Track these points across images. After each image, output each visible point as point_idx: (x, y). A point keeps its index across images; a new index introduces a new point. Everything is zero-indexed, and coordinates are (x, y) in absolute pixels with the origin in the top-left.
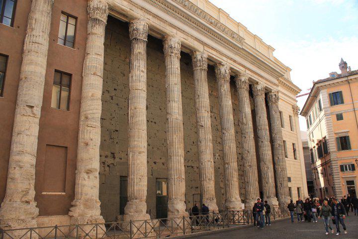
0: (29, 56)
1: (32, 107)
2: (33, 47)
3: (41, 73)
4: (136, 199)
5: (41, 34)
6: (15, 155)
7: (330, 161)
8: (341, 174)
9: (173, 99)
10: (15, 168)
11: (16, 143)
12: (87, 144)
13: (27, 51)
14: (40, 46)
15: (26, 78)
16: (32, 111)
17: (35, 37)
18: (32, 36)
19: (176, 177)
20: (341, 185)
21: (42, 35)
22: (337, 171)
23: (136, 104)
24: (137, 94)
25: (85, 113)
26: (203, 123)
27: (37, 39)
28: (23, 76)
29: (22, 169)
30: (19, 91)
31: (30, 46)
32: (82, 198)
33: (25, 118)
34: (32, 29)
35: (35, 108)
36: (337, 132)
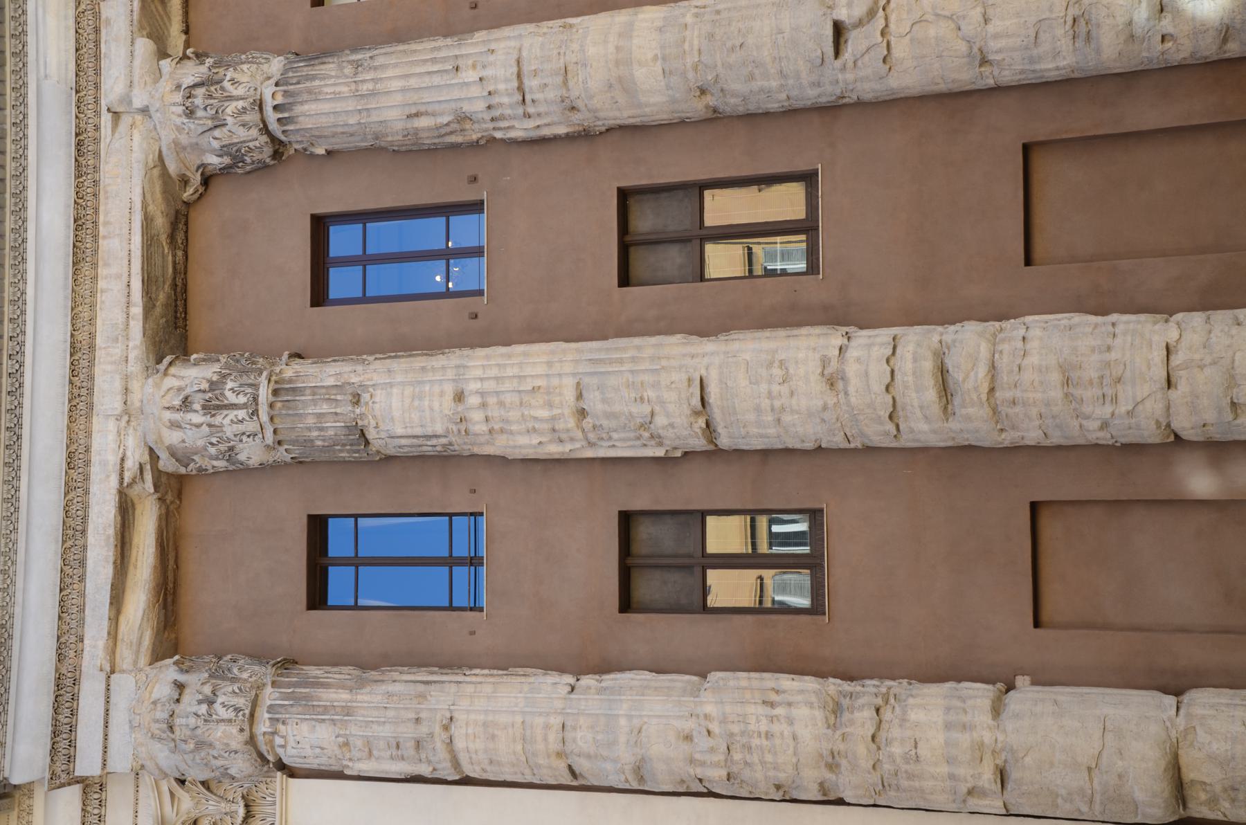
0: (596, 103)
1: (839, 30)
2: (545, 93)
3: (660, 30)
5: (470, 76)
6: (1098, 51)
10: (1163, 37)
11: (1032, 60)
13: (576, 117)
14: (526, 68)
15: (703, 91)
16: (860, 23)
17: (495, 100)
18: (496, 113)
21: (474, 66)
27: (502, 87)
28: (696, 108)
30: (773, 106)
31: (542, 109)
33: (899, 51)
34: (463, 118)
35: (842, 14)
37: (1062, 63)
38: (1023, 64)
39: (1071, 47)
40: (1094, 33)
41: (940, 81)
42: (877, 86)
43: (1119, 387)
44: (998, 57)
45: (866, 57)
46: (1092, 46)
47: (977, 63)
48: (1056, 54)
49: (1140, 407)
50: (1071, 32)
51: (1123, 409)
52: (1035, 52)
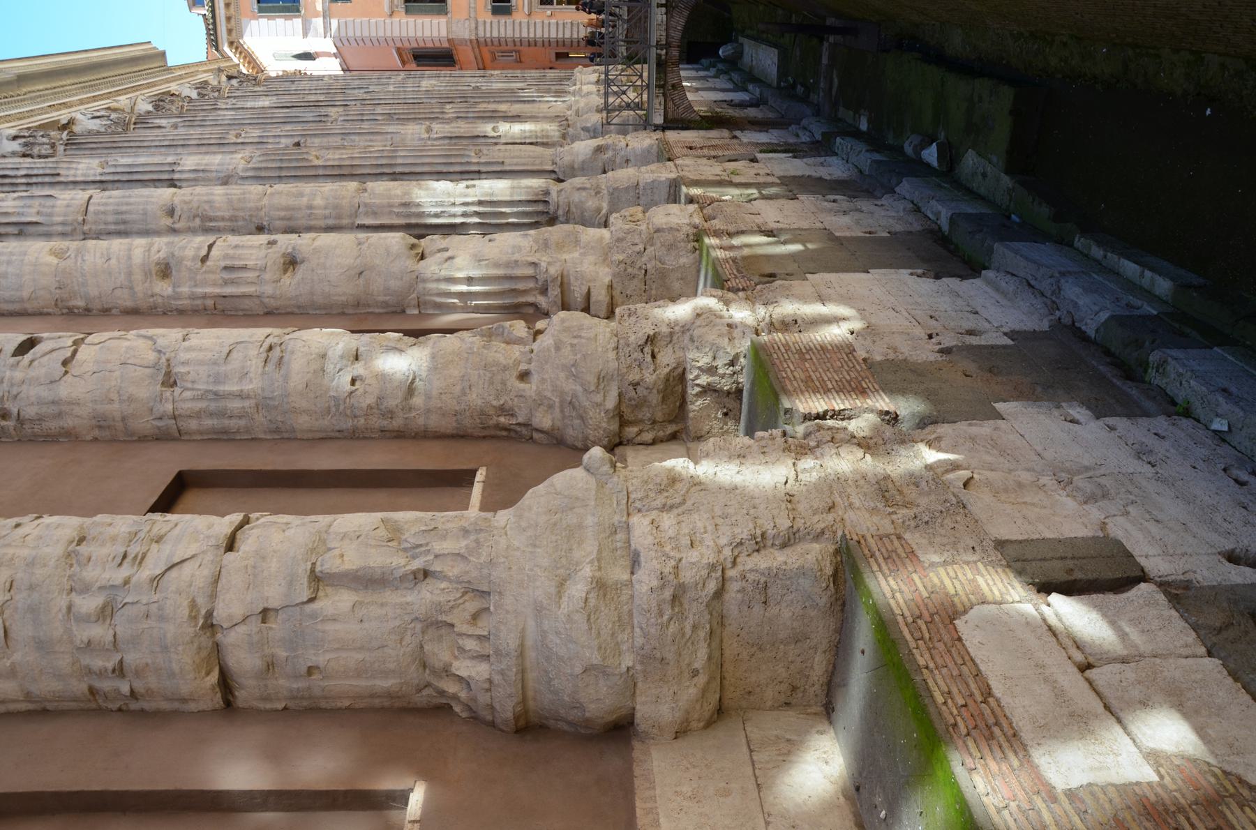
4: (547, 193)
6: (286, 378)
7: (478, 44)
8: (519, 17)
9: (167, 168)
11: (217, 381)
12: (291, 262)
19: (475, 160)
20: (553, 21)
22: (510, 28)
23: (149, 207)
24: (106, 204)
25: (138, 276)
26: (283, 140)
29: (362, 349)
32: (530, 259)
36: (387, 9)
37: (247, 387)
38: (207, 383)
39: (260, 370)
40: (285, 359)
41: (115, 396)
42: (45, 393)
43: (155, 547)
44: (182, 369)
45: (46, 358)
46: (282, 372)
47: (161, 378)
48: (244, 375)
49: (174, 573)
50: (265, 355)
51: (147, 572)
52: (223, 369)
